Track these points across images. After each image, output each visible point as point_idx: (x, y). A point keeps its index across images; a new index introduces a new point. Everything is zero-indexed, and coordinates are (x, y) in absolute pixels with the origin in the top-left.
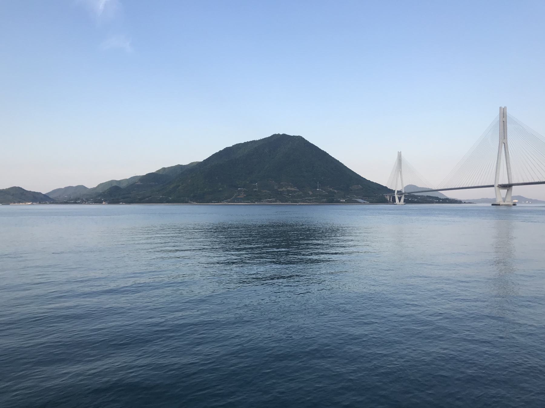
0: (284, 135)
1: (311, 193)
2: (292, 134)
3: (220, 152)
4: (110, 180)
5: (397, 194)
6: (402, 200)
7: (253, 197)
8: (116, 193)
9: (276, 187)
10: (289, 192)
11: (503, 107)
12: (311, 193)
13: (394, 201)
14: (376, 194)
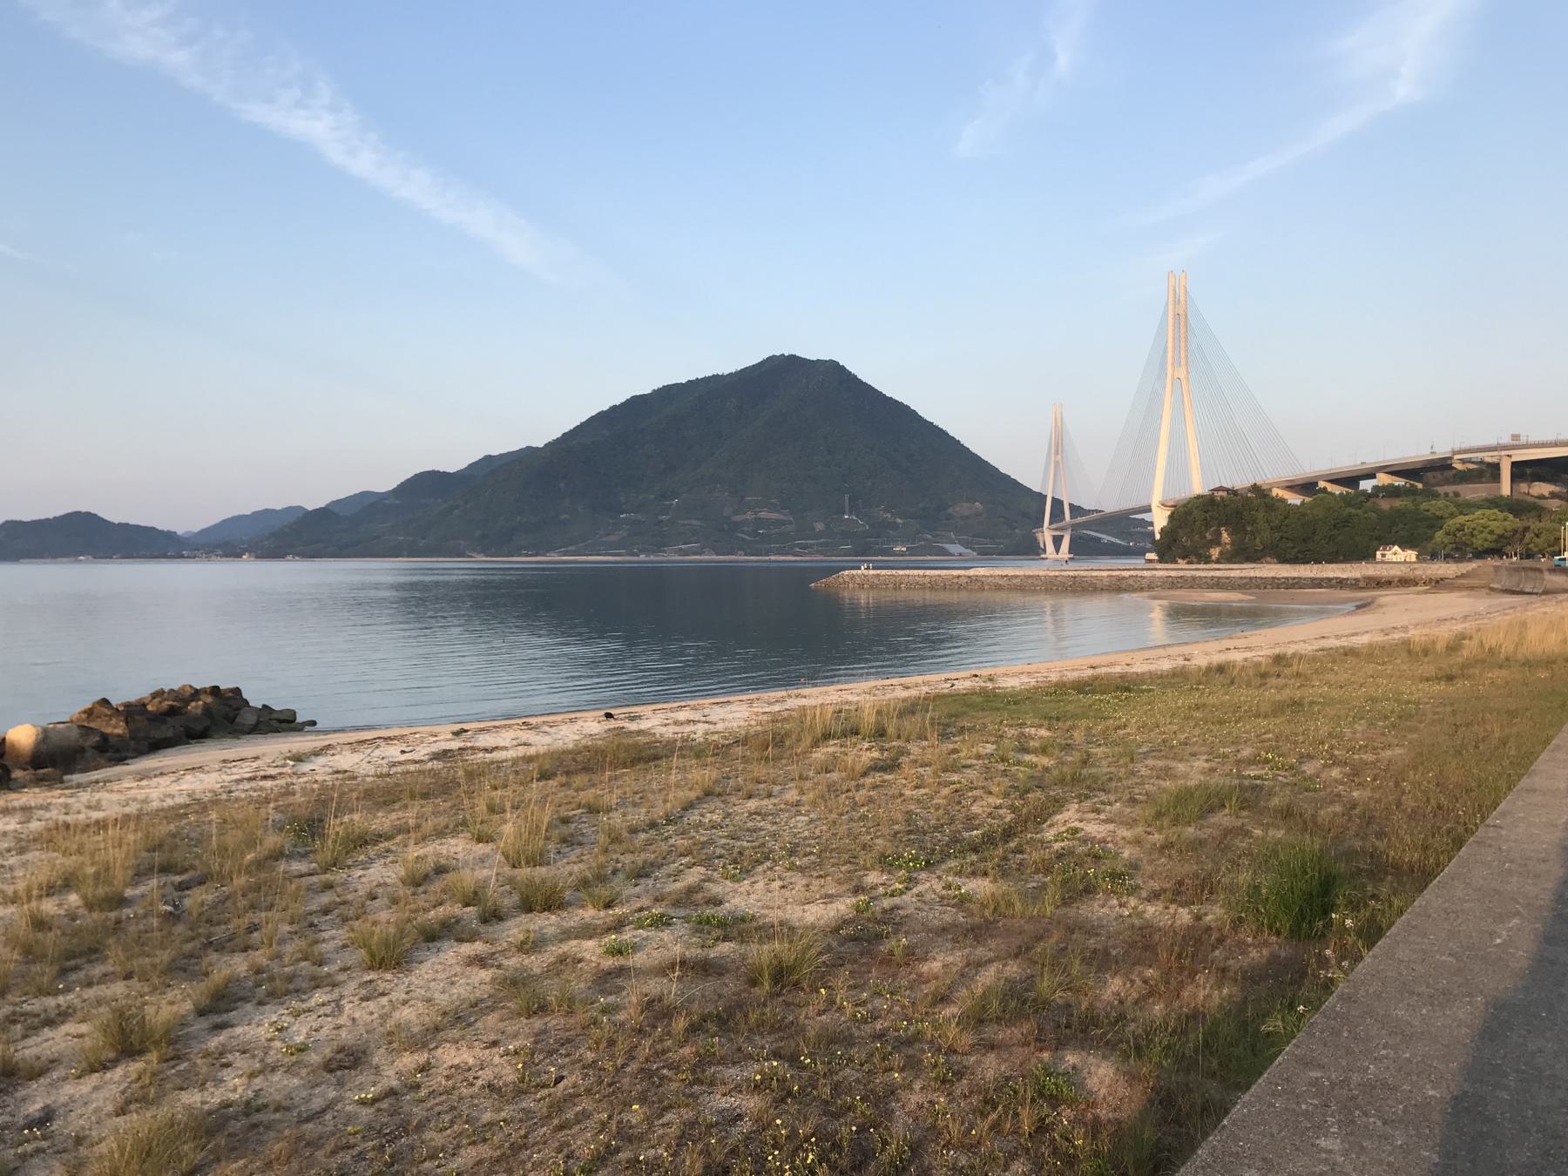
1: (819, 526)
2: (812, 356)
3: (614, 408)
9: (727, 511)
10: (760, 522)
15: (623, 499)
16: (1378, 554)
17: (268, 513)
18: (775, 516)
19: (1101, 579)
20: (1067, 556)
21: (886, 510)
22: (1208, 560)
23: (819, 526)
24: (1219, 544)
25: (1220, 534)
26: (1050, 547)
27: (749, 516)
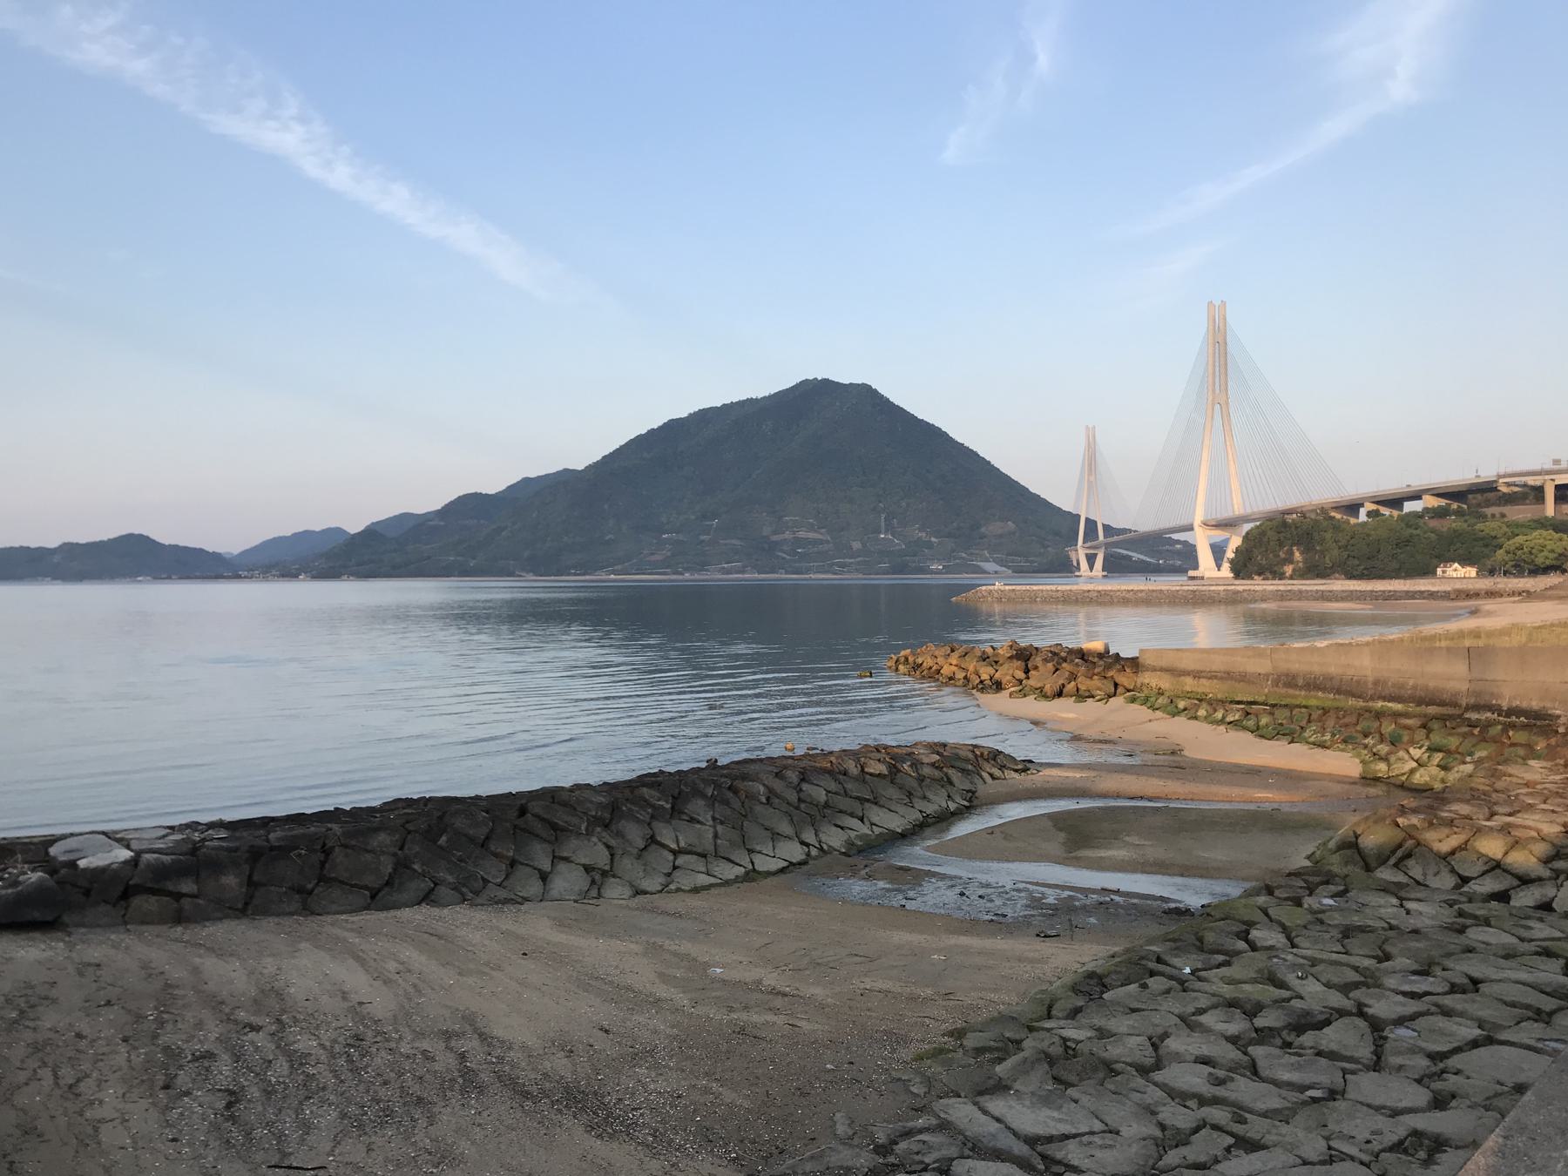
0: (826, 381)
1: (856, 545)
3: (651, 432)
4: (397, 513)
9: (766, 531)
10: (798, 542)
11: (1217, 303)
15: (664, 519)
16: (1439, 571)
17: (307, 534)
18: (811, 535)
19: (1218, 593)
20: (1101, 574)
21: (920, 530)
22: (1282, 576)
23: (856, 545)
24: (1291, 562)
25: (1292, 554)
26: (1084, 565)
27: (788, 535)
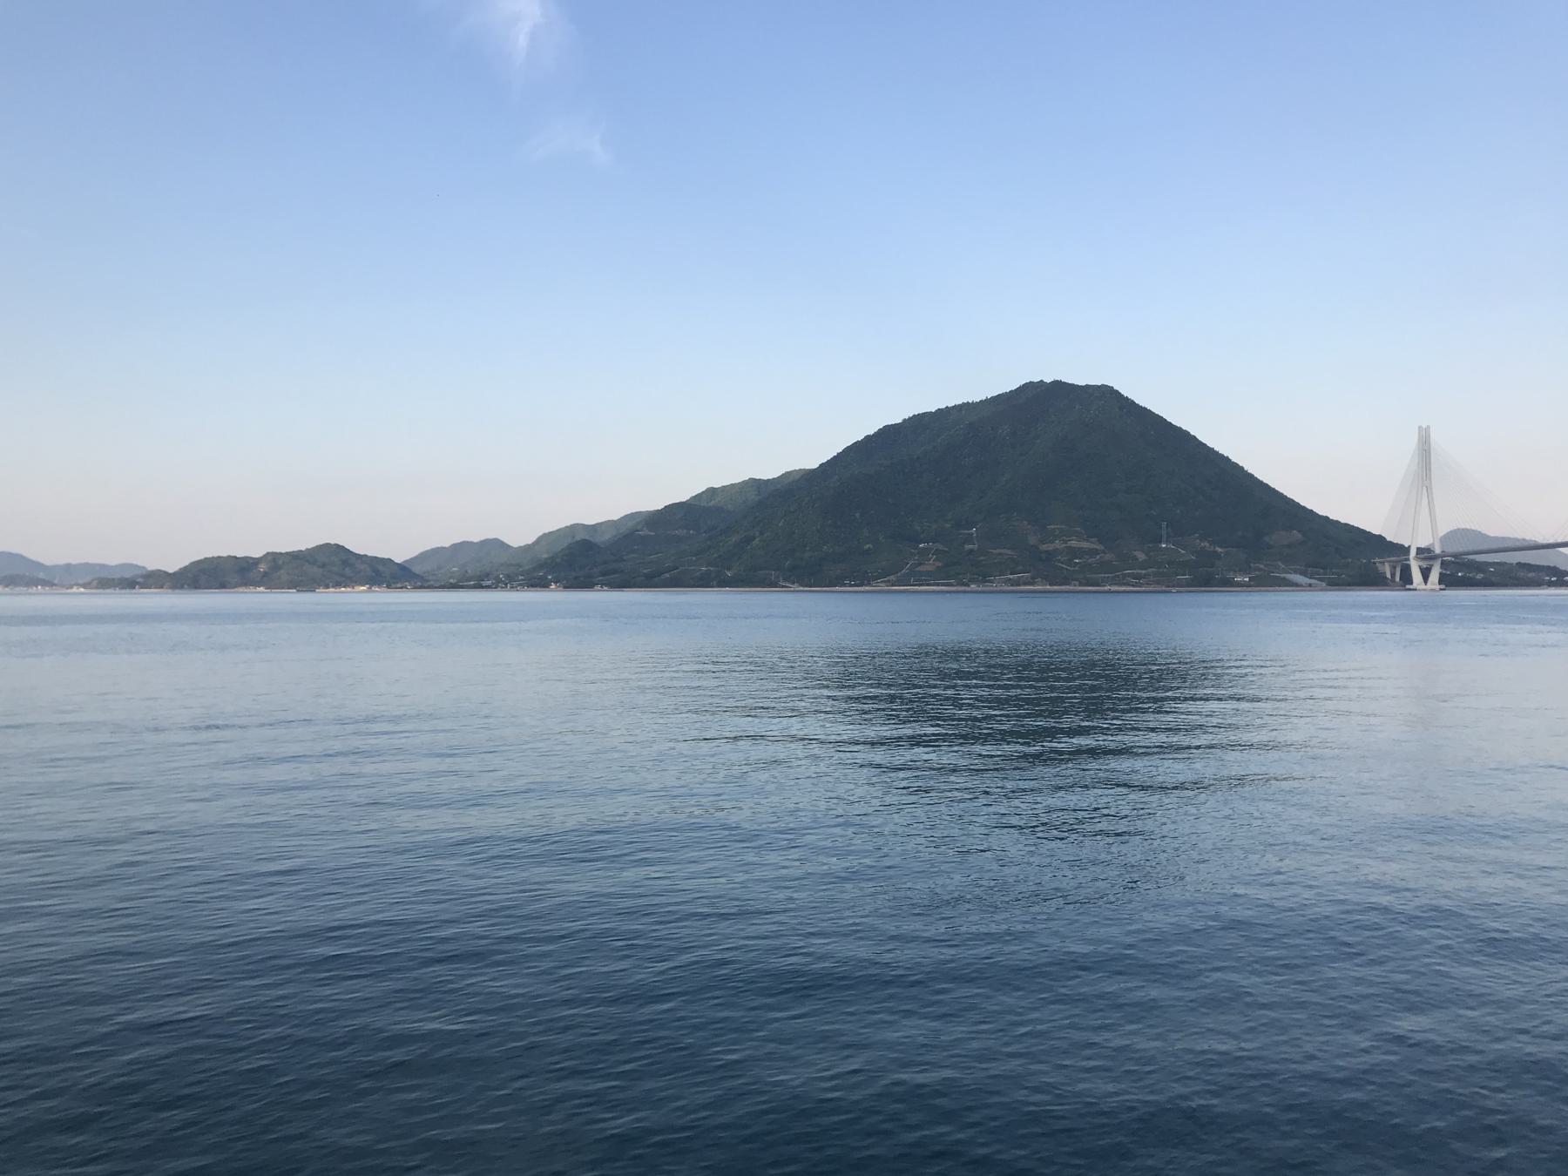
0: (1058, 384)
1: (1141, 556)
2: (1080, 380)
5: (1417, 558)
6: (1434, 576)
7: (964, 570)
8: (587, 561)
9: (1032, 540)
10: (1074, 553)
12: (1141, 556)
13: (1407, 578)
14: (1348, 559)
18: (1085, 545)
27: (1058, 544)
